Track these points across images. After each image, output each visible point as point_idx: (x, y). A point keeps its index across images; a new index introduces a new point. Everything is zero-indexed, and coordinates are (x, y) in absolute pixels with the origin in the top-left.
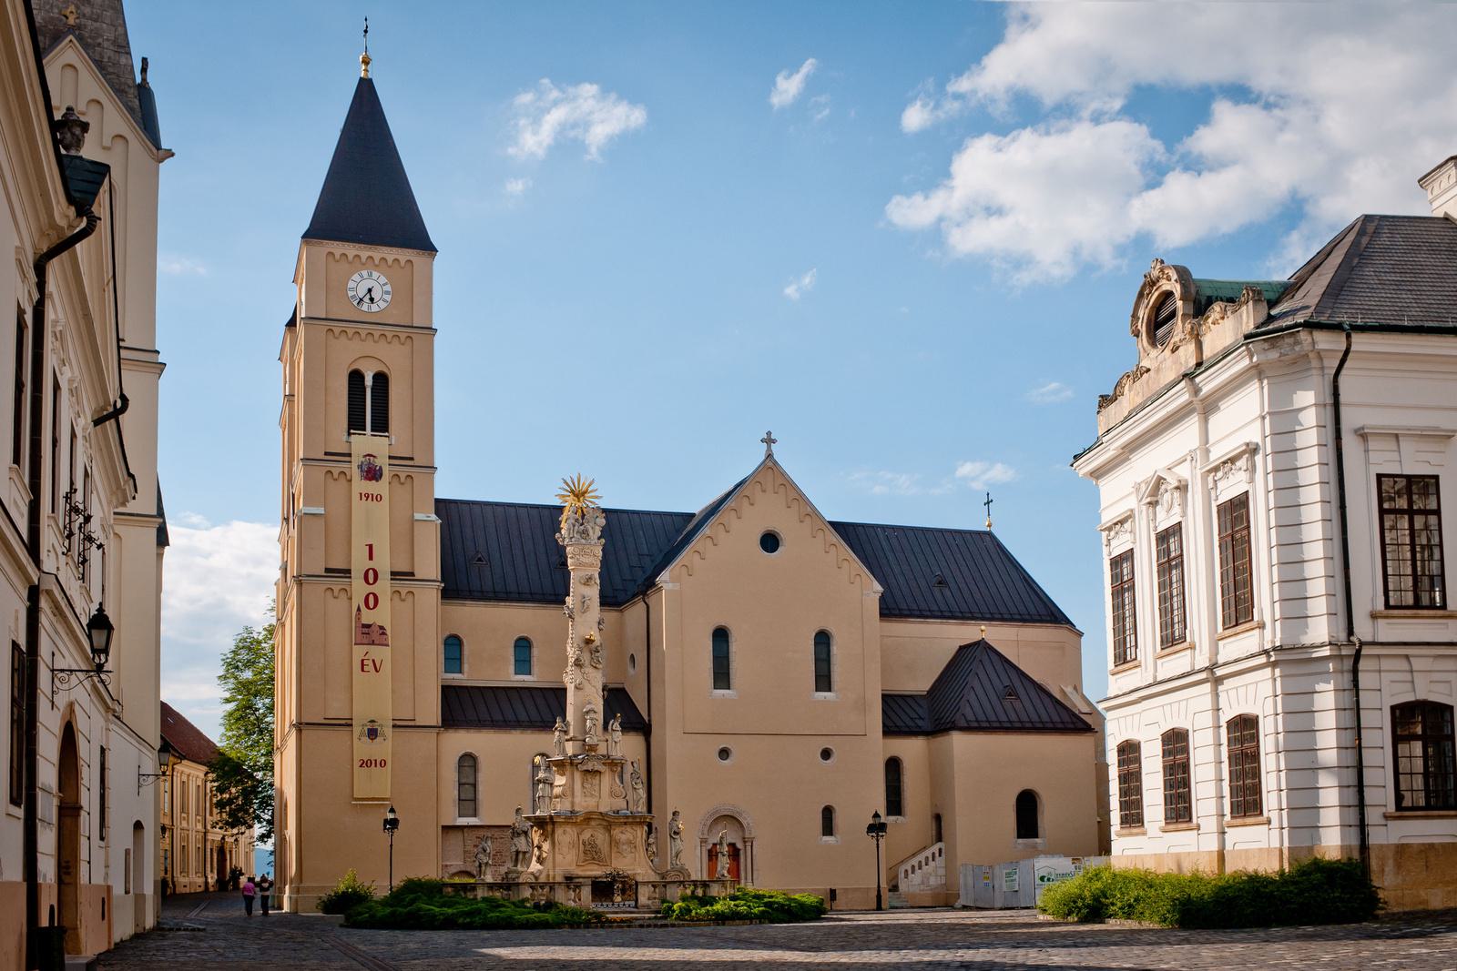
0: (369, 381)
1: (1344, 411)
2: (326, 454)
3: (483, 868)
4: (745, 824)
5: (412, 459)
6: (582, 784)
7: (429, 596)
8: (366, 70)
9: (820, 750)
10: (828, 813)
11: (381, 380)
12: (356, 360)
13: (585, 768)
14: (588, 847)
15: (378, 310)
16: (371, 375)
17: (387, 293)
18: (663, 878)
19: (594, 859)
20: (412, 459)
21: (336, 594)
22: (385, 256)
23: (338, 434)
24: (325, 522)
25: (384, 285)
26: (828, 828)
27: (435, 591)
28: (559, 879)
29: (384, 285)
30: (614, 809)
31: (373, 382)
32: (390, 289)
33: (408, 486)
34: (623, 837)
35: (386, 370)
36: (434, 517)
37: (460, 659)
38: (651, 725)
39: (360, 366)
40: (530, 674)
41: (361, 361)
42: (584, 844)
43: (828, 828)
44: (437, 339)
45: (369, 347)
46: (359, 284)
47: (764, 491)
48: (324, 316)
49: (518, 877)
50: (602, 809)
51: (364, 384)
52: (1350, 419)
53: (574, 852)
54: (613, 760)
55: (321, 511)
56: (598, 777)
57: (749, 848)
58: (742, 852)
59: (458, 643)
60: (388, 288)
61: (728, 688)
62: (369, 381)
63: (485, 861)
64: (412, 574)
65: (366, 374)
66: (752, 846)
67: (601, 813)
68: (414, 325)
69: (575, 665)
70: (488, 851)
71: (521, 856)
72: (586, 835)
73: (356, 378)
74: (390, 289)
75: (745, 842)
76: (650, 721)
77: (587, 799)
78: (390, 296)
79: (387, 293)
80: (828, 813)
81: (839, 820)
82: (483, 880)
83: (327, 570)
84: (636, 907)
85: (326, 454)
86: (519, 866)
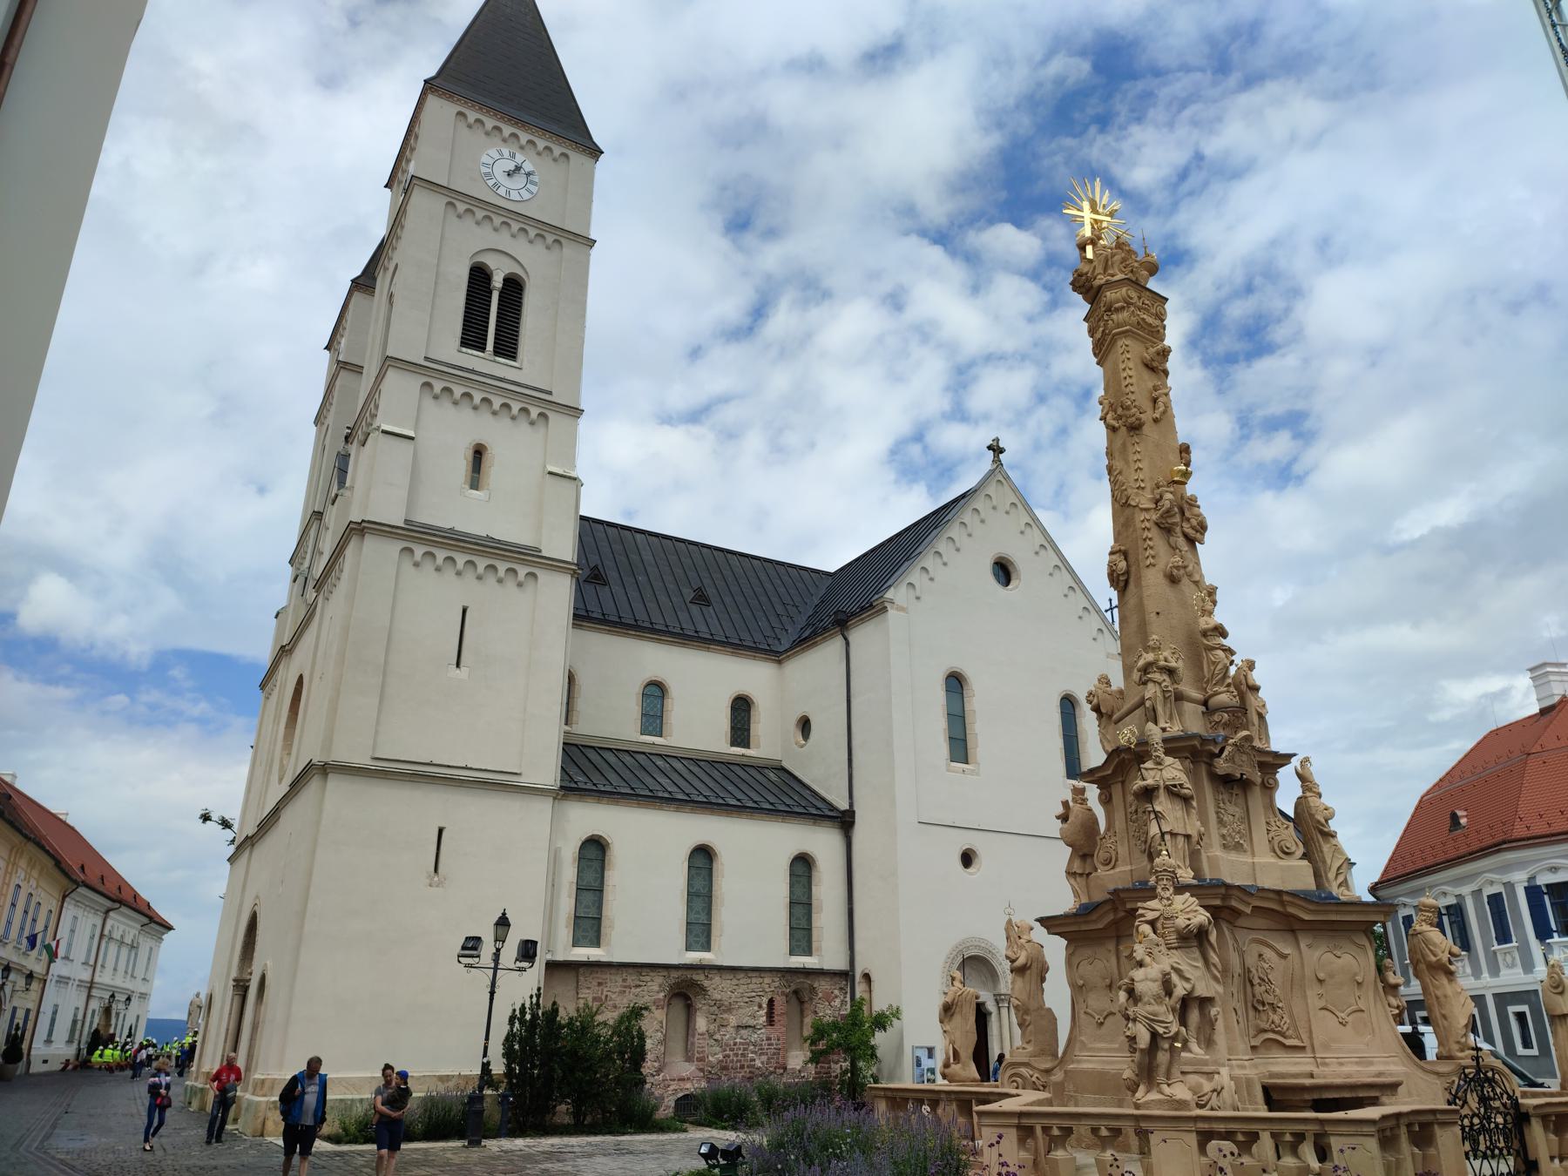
0: (497, 282)
11: (514, 287)
12: (477, 253)
15: (519, 199)
20: (550, 393)
24: (415, 447)
31: (503, 284)
35: (524, 276)
38: (853, 813)
40: (661, 736)
44: (595, 252)
45: (503, 240)
51: (489, 284)
55: (412, 434)
62: (497, 282)
73: (479, 277)
83: (406, 522)
85: (426, 359)
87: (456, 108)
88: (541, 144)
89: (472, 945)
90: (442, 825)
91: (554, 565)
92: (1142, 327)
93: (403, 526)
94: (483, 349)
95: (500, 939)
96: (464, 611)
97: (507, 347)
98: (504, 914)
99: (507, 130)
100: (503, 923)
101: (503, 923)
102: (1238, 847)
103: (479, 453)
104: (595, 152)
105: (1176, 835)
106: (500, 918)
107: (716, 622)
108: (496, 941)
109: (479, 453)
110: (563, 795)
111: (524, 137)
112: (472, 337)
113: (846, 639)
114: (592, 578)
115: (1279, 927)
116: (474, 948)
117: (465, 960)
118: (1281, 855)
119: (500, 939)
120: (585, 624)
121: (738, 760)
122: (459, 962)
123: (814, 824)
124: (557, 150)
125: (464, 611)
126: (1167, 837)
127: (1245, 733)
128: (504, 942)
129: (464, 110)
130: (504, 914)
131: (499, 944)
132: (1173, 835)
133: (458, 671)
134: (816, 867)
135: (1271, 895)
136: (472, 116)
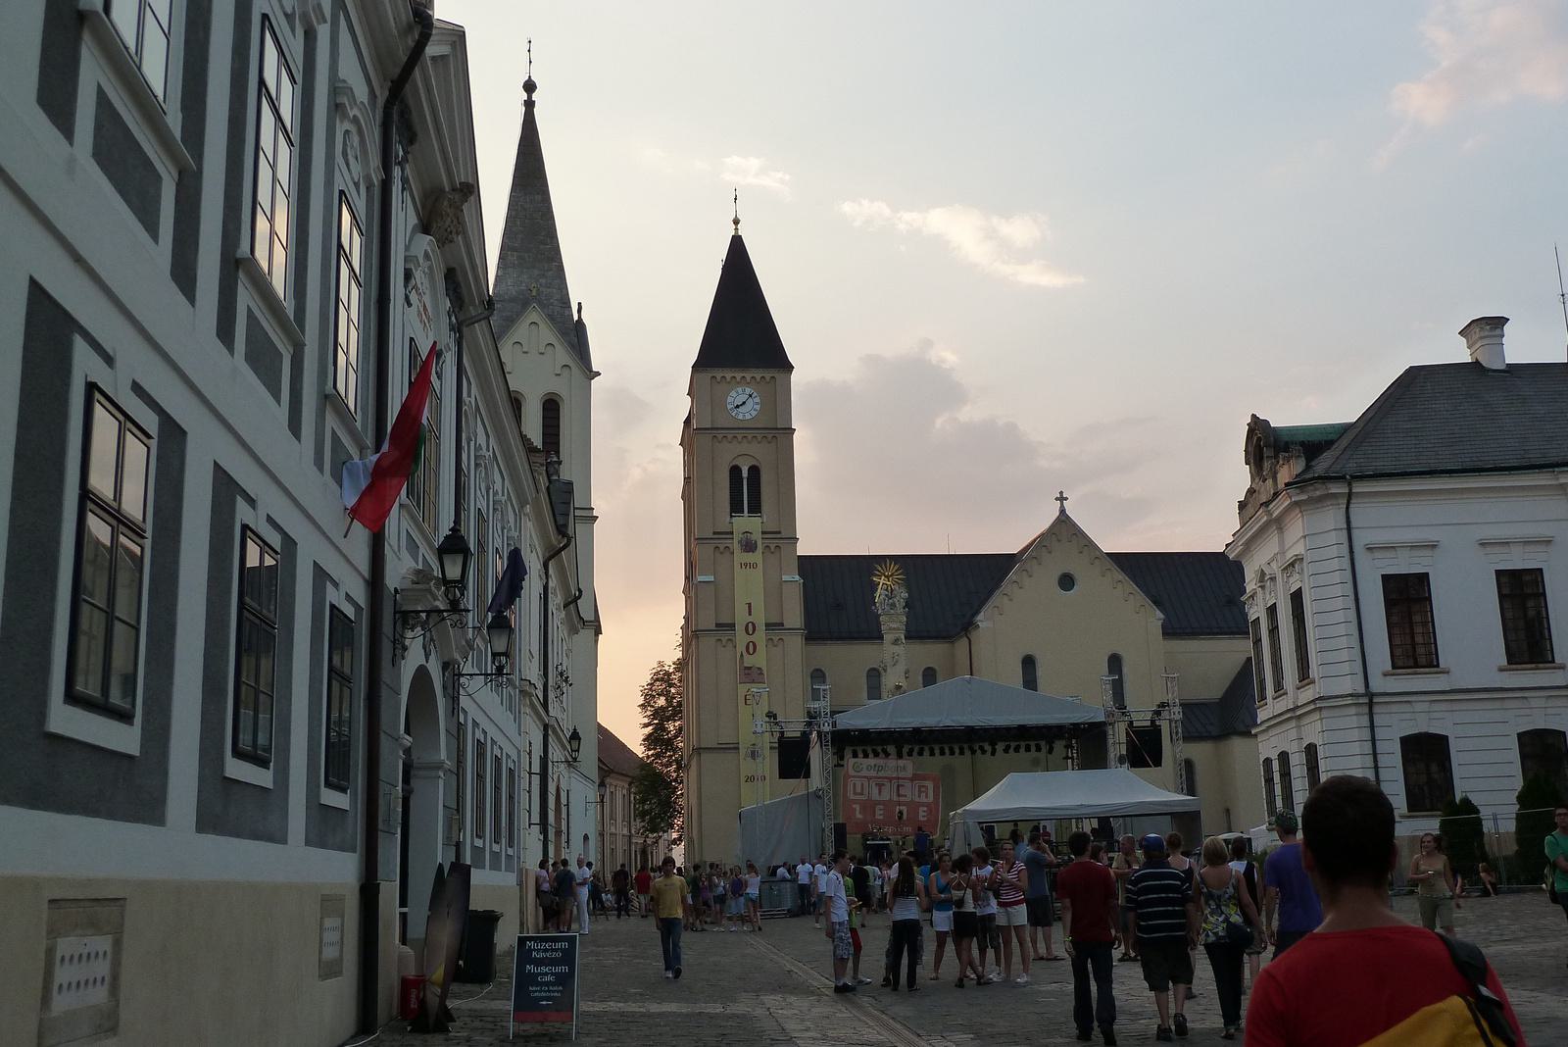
0: (745, 474)
1: (1355, 533)
2: (714, 533)
5: (779, 533)
7: (795, 643)
8: (736, 229)
11: (754, 471)
17: (757, 403)
20: (779, 533)
22: (755, 375)
23: (724, 519)
35: (758, 465)
36: (797, 578)
39: (738, 462)
46: (736, 396)
47: (1059, 541)
48: (710, 426)
52: (1361, 539)
62: (745, 474)
64: (782, 625)
68: (779, 427)
73: (735, 471)
79: (757, 403)
83: (717, 625)
85: (714, 533)
97: (755, 508)
99: (739, 376)
111: (748, 376)
112: (736, 507)
113: (968, 638)
124: (768, 376)
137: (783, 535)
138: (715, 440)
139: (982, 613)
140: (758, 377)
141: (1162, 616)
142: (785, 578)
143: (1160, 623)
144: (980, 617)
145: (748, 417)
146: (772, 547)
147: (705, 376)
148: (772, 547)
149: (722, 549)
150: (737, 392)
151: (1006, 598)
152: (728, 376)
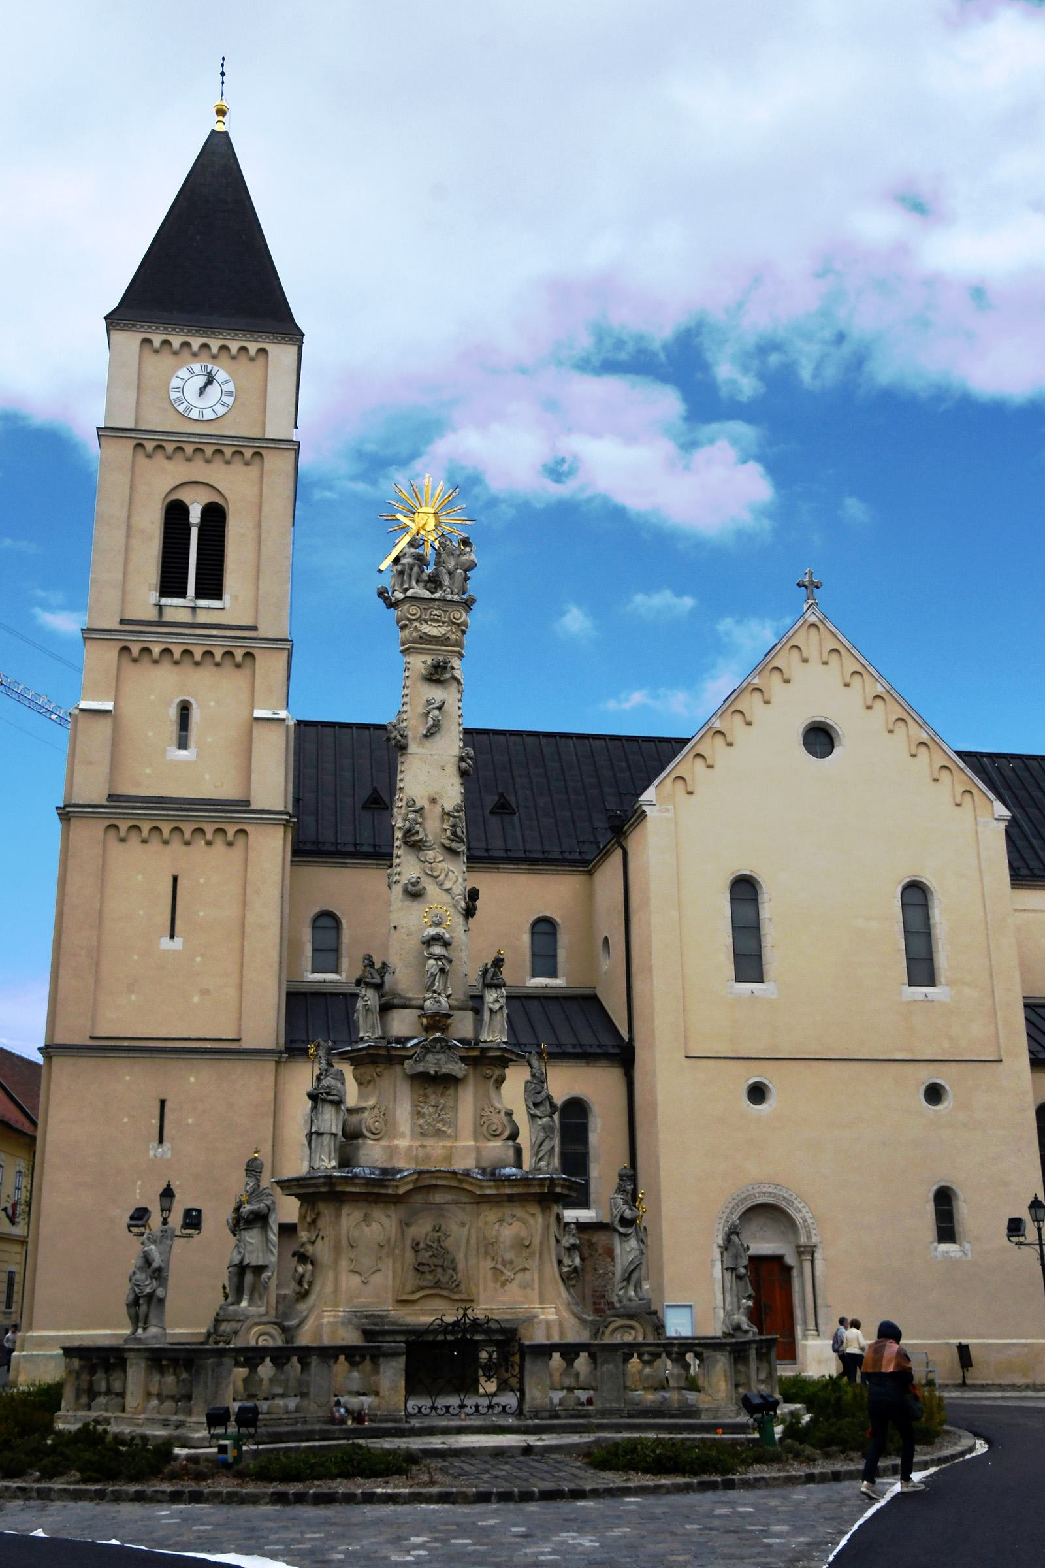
0: (195, 516)
3: (143, 1309)
4: (798, 1218)
6: (414, 1106)
9: (924, 1087)
10: (944, 1199)
11: (215, 516)
13: (420, 1068)
14: (425, 1256)
15: (213, 416)
16: (200, 508)
17: (228, 394)
18: (595, 1334)
19: (437, 1284)
21: (123, 833)
25: (225, 382)
26: (946, 1231)
27: (282, 829)
28: (351, 1337)
29: (225, 382)
30: (484, 1164)
32: (233, 389)
33: (246, 671)
34: (508, 1232)
37: (336, 950)
38: (633, 1049)
39: (185, 496)
41: (188, 489)
42: (416, 1247)
43: (946, 1231)
45: (197, 470)
48: (132, 426)
49: (236, 1333)
50: (459, 1166)
51: (188, 520)
53: (388, 1266)
54: (483, 1050)
55: (109, 706)
56: (451, 1091)
57: (807, 1265)
58: (795, 1273)
59: (333, 924)
60: (230, 387)
61: (761, 980)
62: (195, 516)
63: (148, 1290)
64: (247, 803)
65: (191, 508)
66: (812, 1261)
67: (454, 1173)
69: (405, 843)
70: (155, 1265)
71: (249, 1278)
72: (422, 1229)
73: (175, 513)
74: (233, 389)
75: (800, 1254)
76: (631, 1039)
77: (429, 1142)
78: (233, 398)
79: (228, 394)
80: (944, 1199)
81: (964, 1210)
82: (139, 1340)
83: (111, 797)
84: (520, 1412)
85: (122, 622)
86: (244, 1304)
87: (140, 336)
88: (234, 346)
89: (140, 1216)
90: (162, 1097)
91: (265, 817)
92: (427, 640)
93: (105, 803)
94: (183, 594)
95: (166, 1209)
96: (175, 879)
97: (211, 586)
98: (169, 1185)
99: (196, 343)
100: (168, 1194)
101: (168, 1194)
102: (439, 1133)
103: (185, 709)
104: (295, 335)
105: (322, 1134)
106: (165, 1189)
107: (518, 833)
108: (162, 1210)
109: (185, 709)
110: (288, 1058)
111: (215, 344)
112: (172, 584)
114: (372, 803)
115: (472, 1201)
116: (140, 1218)
117: (135, 1230)
118: (491, 1138)
119: (166, 1209)
120: (348, 861)
121: (541, 992)
122: (130, 1231)
123: (588, 1064)
124: (253, 347)
125: (175, 879)
126: (314, 1136)
127: (438, 1035)
128: (170, 1211)
129: (148, 336)
130: (169, 1185)
131: (166, 1214)
132: (320, 1134)
133: (171, 943)
134: (591, 1111)
135: (448, 1175)
136: (157, 339)
137: (262, 633)
138: (140, 452)
139: (652, 789)
140: (234, 346)
141: (1006, 813)
142: (258, 713)
143: (1002, 826)
144: (649, 795)
145: (209, 416)
146: (239, 654)
147: (130, 340)
148: (239, 654)
149: (135, 650)
150: (191, 371)
151: (699, 763)
152: (176, 341)
